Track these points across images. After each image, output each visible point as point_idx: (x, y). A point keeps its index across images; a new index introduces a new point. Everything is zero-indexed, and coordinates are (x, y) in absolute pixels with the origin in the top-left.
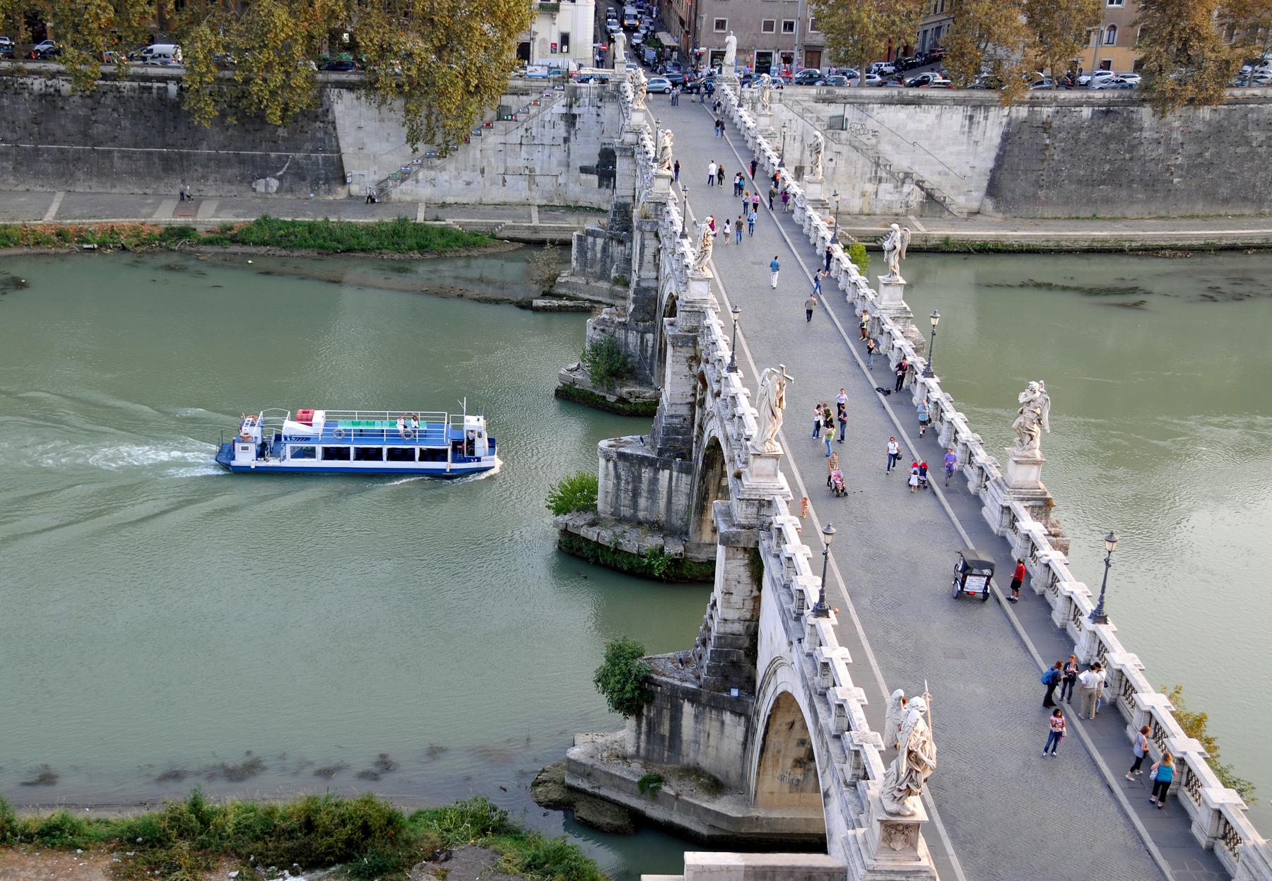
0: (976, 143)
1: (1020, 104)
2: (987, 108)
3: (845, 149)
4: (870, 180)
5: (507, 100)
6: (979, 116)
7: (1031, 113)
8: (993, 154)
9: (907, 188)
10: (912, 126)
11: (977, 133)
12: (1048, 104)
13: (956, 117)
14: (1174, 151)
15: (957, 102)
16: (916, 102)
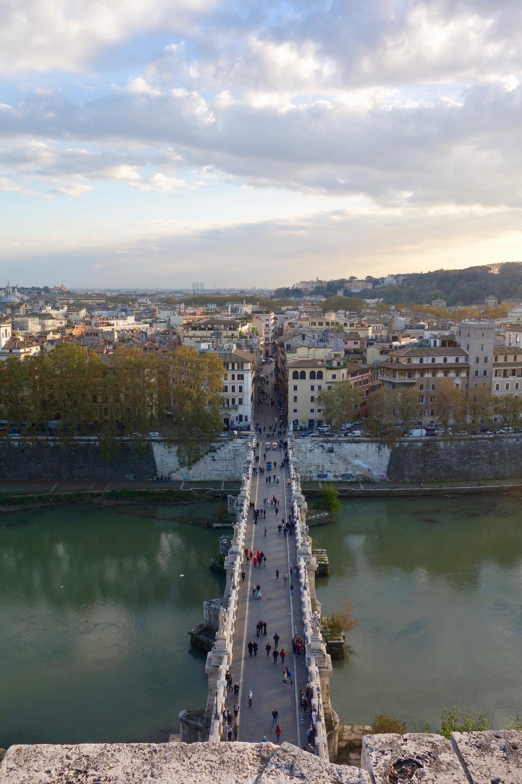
0: (381, 456)
2: (384, 444)
5: (213, 444)
8: (388, 459)
11: (382, 452)
12: (406, 442)
14: (453, 457)
15: (372, 442)
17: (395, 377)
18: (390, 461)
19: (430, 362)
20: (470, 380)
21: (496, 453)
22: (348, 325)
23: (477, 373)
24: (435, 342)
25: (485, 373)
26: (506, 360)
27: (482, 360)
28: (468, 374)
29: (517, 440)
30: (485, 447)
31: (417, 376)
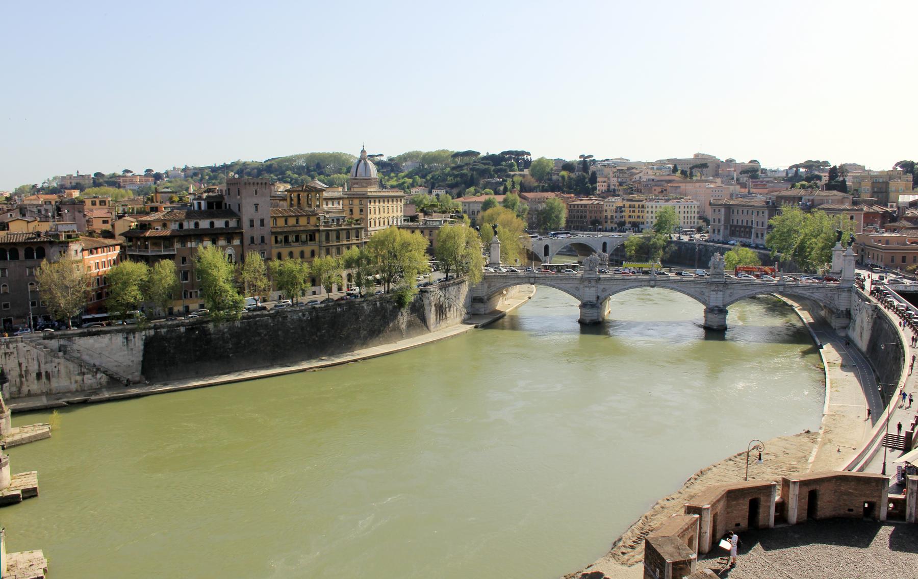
1: (150, 328)
2: (134, 333)
3: (62, 361)
4: (79, 374)
6: (131, 337)
7: (156, 333)
8: (141, 354)
9: (99, 376)
10: (97, 345)
11: (131, 345)
13: (119, 339)
15: (118, 331)
16: (98, 333)
17: (146, 247)
18: (144, 355)
19: (192, 226)
20: (245, 248)
21: (280, 333)
22: (98, 203)
23: (252, 238)
24: (199, 204)
25: (263, 238)
26: (286, 223)
27: (257, 223)
28: (242, 242)
29: (304, 315)
30: (266, 326)
31: (177, 246)
